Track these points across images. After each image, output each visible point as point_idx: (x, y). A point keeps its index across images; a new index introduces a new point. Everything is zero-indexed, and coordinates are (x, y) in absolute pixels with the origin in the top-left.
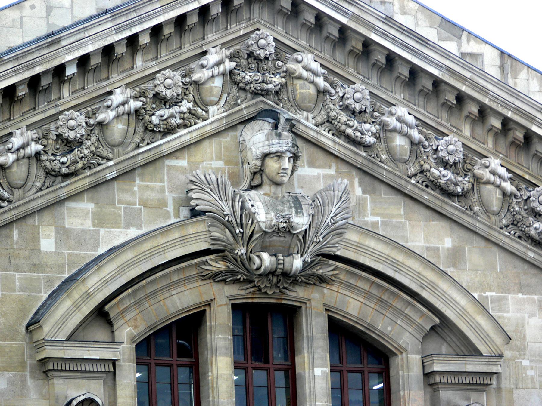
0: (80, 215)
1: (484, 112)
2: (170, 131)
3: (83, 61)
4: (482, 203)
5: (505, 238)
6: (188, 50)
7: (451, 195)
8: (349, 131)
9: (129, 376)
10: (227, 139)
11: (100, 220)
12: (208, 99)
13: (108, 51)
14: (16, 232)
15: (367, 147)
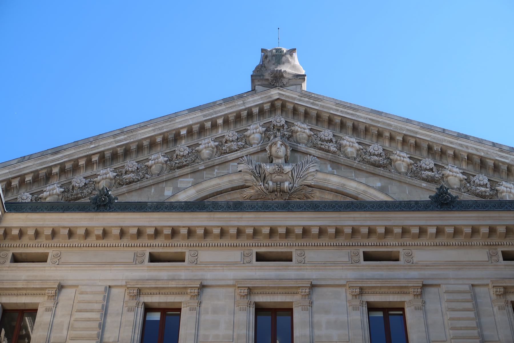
2: (232, 151)
5: (408, 180)
7: (379, 166)
8: (323, 146)
12: (252, 142)
14: (153, 190)
15: (334, 153)
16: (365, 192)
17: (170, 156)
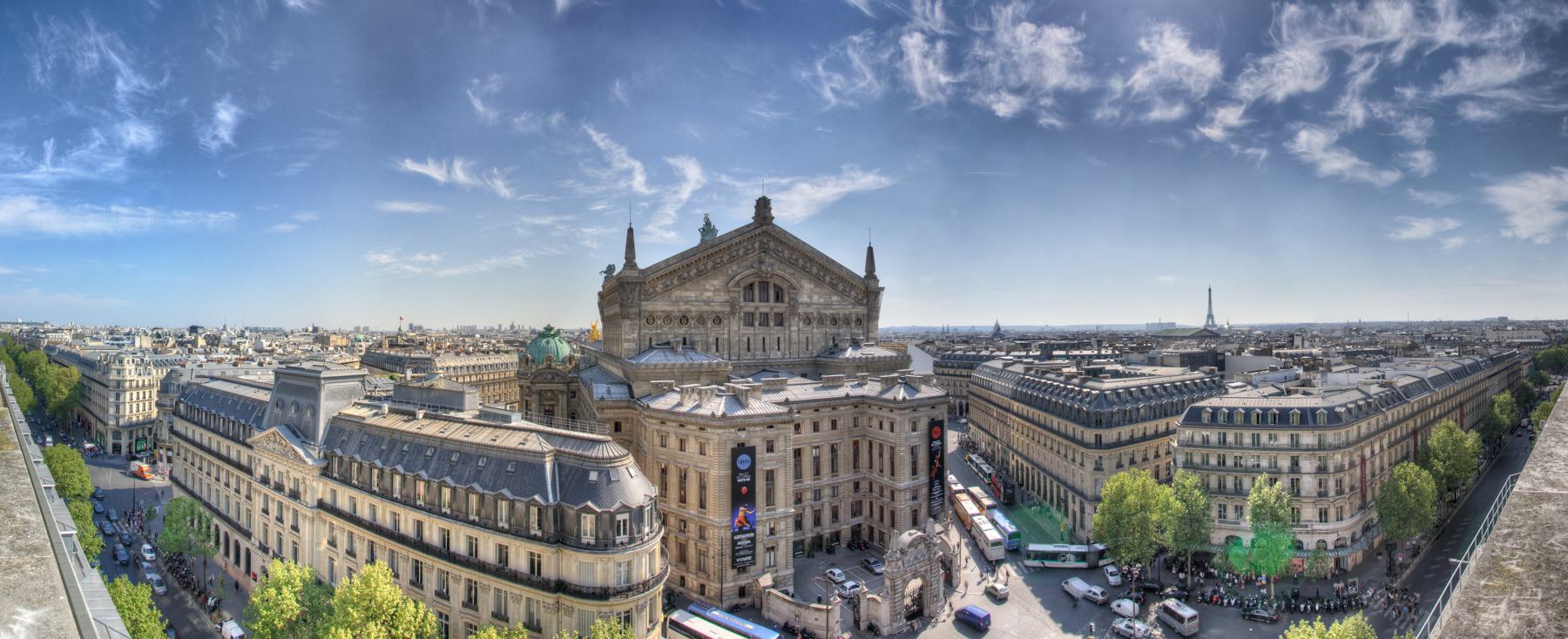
0: (735, 267)
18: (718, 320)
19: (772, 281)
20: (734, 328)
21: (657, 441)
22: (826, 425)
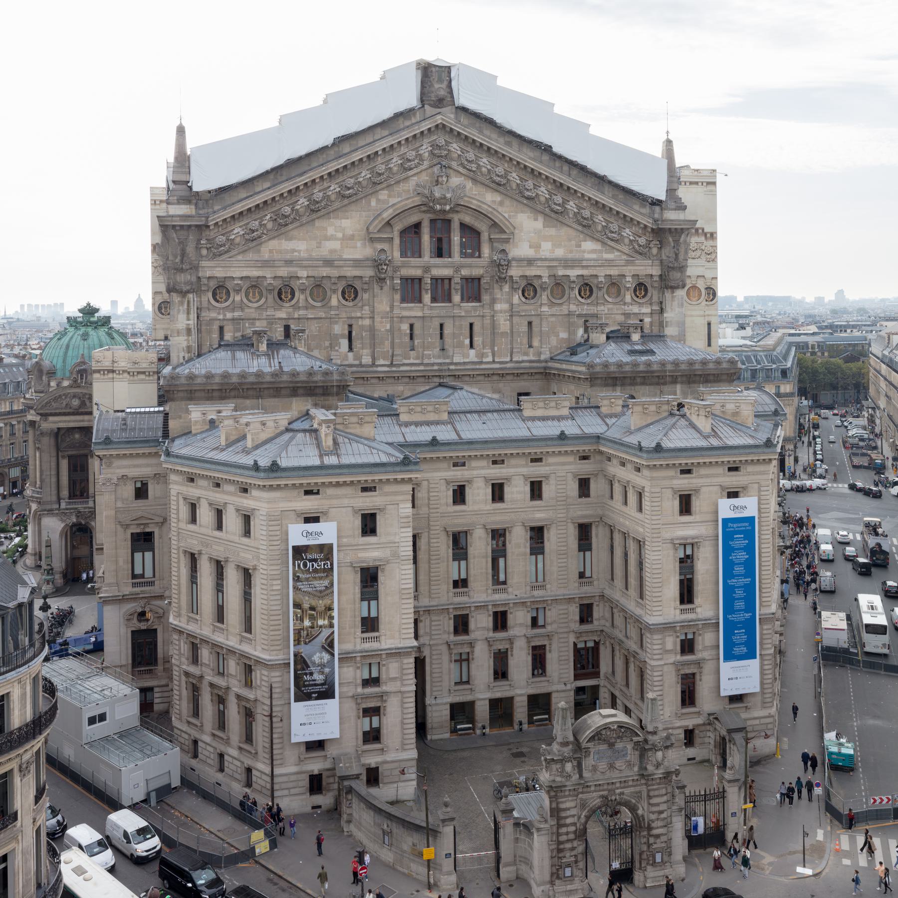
0: (383, 195)
1: (511, 159)
2: (411, 169)
3: (384, 149)
4: (510, 186)
6: (418, 145)
7: (500, 185)
9: (397, 241)
10: (429, 171)
11: (389, 196)
13: (392, 146)
16: (492, 213)
17: (372, 170)
18: (351, 292)
19: (456, 219)
20: (382, 305)
21: (184, 511)
22: (517, 491)
